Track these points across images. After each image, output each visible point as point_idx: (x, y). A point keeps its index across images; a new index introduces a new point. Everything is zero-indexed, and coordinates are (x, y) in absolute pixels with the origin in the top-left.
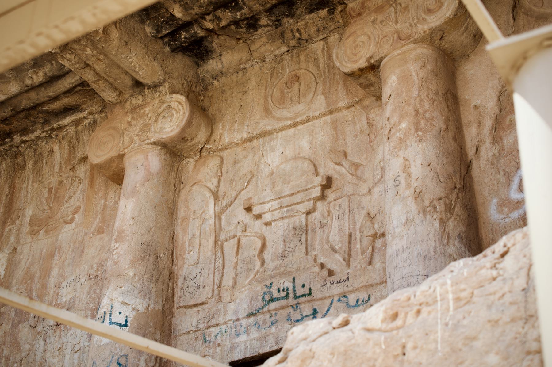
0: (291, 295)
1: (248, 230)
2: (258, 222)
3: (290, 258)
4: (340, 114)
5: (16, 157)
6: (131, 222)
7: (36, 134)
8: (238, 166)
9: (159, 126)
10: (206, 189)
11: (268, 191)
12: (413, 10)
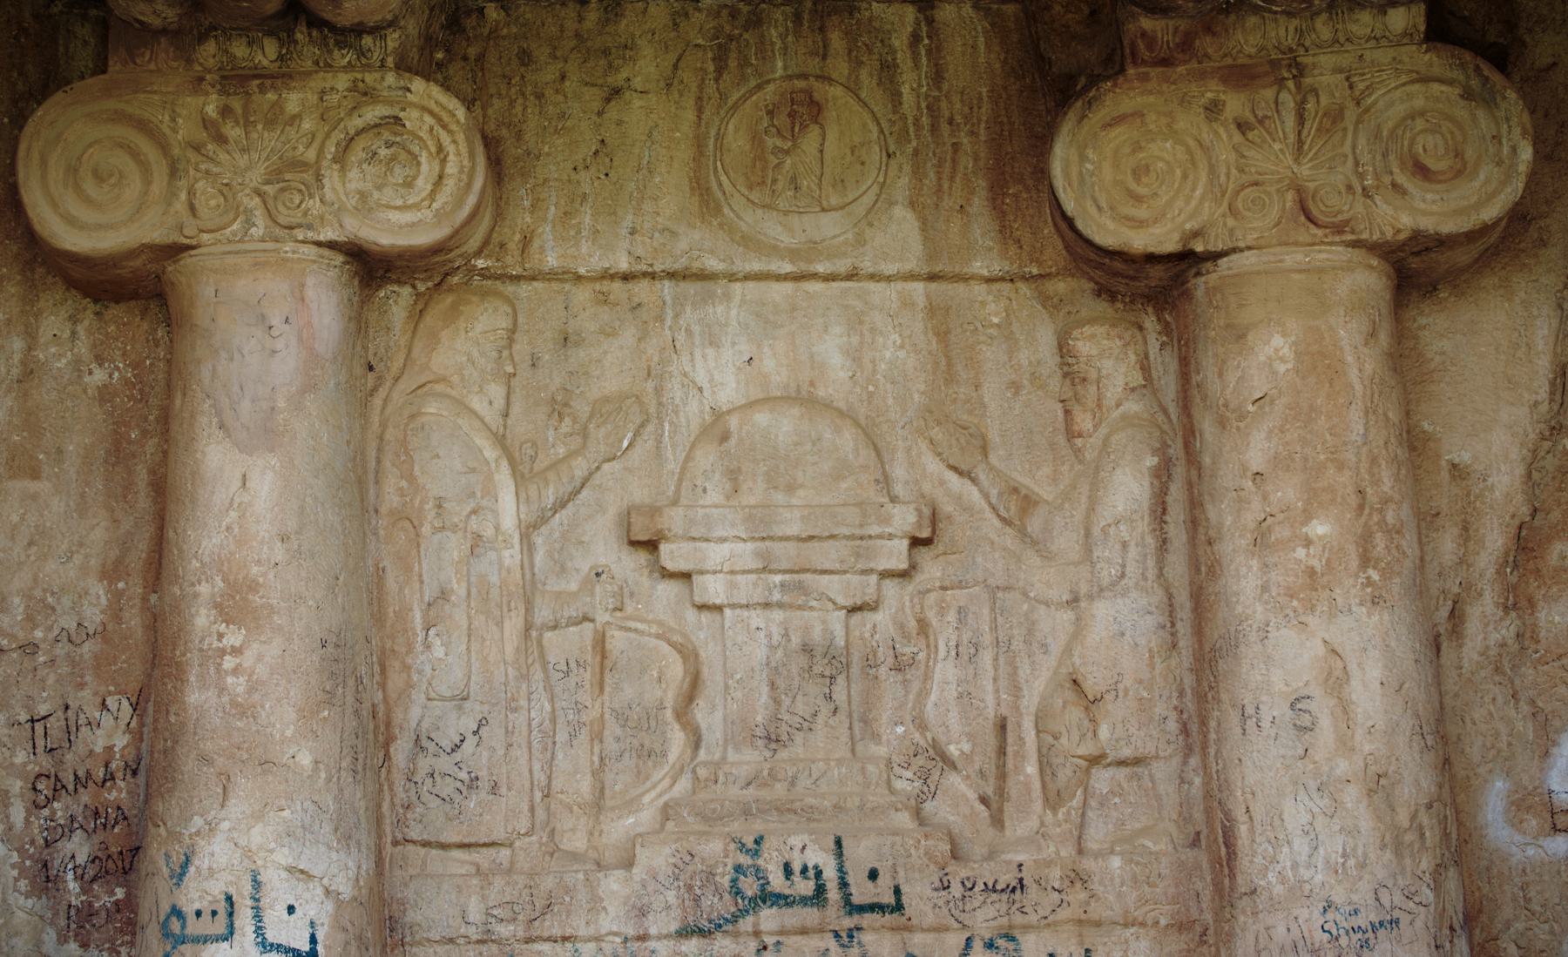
0: (833, 894)
1: (629, 610)
3: (797, 749)
4: (960, 288)
6: (279, 553)
9: (352, 186)
11: (714, 496)
12: (1362, 141)
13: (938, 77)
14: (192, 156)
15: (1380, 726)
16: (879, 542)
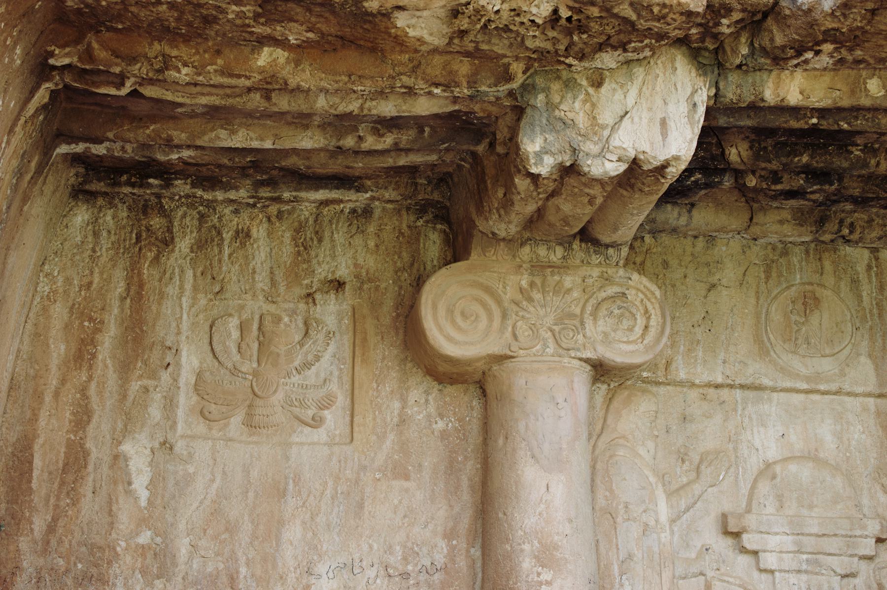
1: (723, 570)
2: (744, 560)
5: (145, 209)
7: (232, 195)
9: (600, 329)
11: (770, 509)
14: (515, 308)
16: (860, 539)
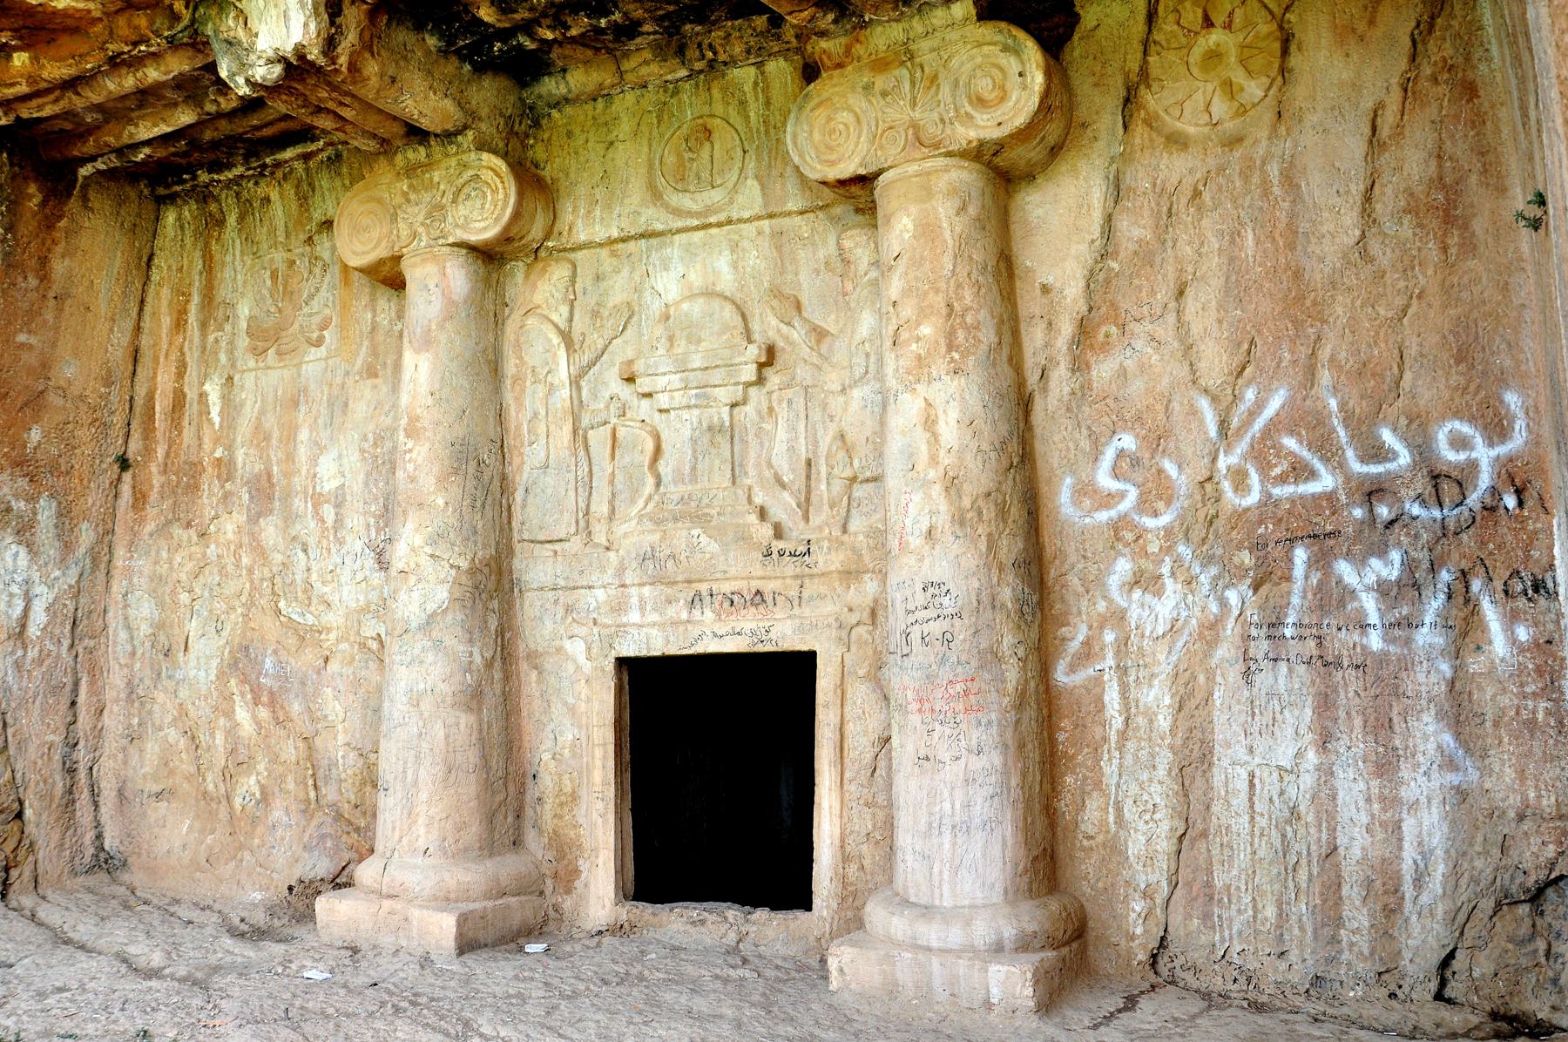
1: (628, 415)
2: (645, 402)
4: (787, 220)
6: (430, 401)
8: (603, 285)
10: (551, 327)
11: (661, 351)
13: (768, 103)
15: (956, 448)
